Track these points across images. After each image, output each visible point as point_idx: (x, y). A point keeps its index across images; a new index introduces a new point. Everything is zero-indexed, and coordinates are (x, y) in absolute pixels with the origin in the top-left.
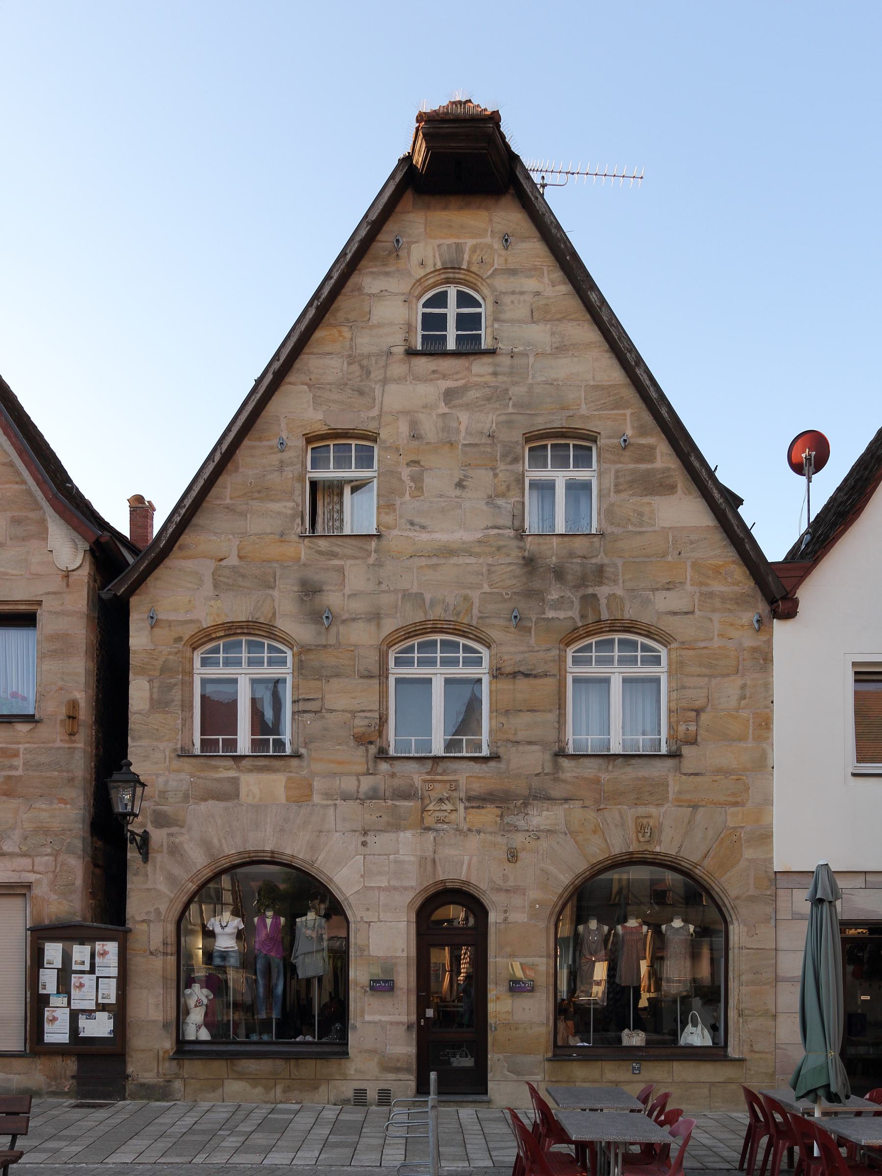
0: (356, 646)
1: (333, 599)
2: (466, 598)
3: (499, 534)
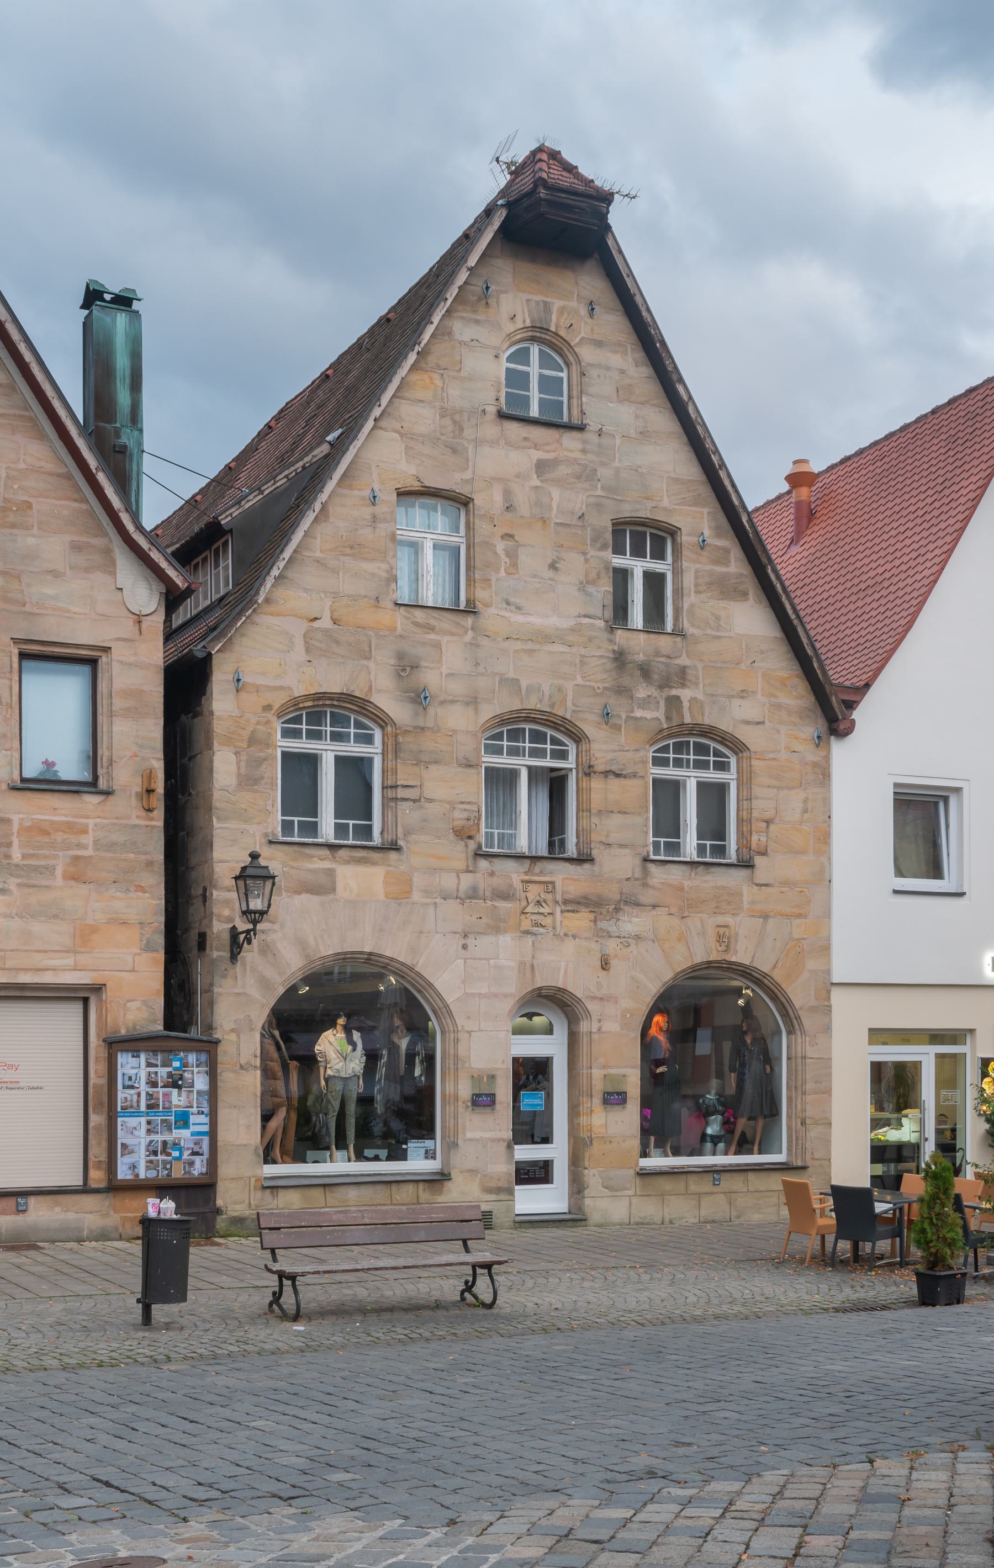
0: (455, 731)
1: (431, 678)
2: (560, 689)
3: (592, 625)
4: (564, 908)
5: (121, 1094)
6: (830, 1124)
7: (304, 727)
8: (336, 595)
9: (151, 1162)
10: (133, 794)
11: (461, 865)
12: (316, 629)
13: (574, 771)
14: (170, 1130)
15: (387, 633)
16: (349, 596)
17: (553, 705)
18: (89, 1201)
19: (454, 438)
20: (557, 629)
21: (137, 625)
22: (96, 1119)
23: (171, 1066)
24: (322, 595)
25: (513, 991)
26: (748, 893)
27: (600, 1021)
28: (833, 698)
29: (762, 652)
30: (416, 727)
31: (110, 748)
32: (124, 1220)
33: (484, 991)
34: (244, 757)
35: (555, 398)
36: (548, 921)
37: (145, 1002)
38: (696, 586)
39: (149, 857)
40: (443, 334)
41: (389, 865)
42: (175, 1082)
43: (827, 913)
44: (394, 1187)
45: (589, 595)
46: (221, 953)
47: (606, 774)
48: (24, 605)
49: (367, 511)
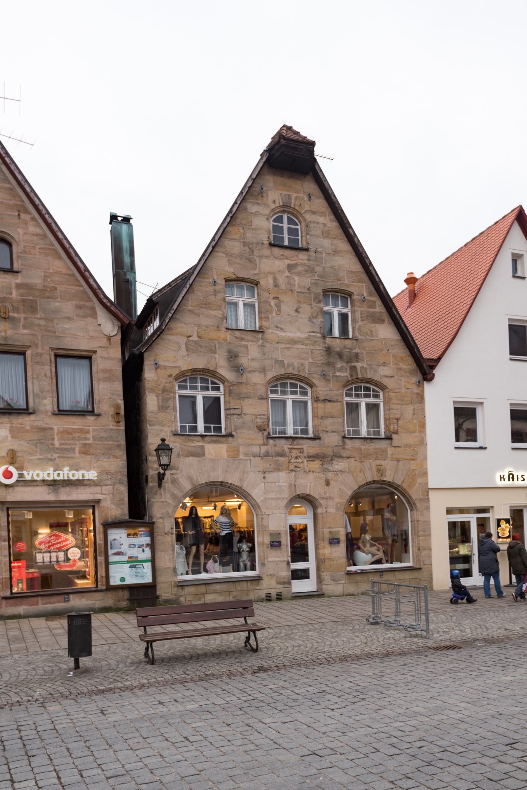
0: (255, 384)
1: (243, 361)
2: (302, 364)
3: (315, 336)
6: (431, 549)
7: (188, 384)
8: (199, 326)
10: (110, 415)
11: (261, 442)
16: (205, 326)
17: (299, 371)
18: (98, 595)
19: (250, 255)
20: (300, 338)
24: (193, 326)
25: (287, 496)
26: (390, 451)
27: (326, 508)
28: (424, 365)
29: (392, 346)
30: (238, 383)
33: (274, 496)
34: (160, 398)
36: (302, 465)
38: (361, 317)
39: (118, 443)
40: (243, 210)
43: (425, 459)
44: (237, 583)
47: (324, 401)
48: (55, 332)
49: (212, 289)
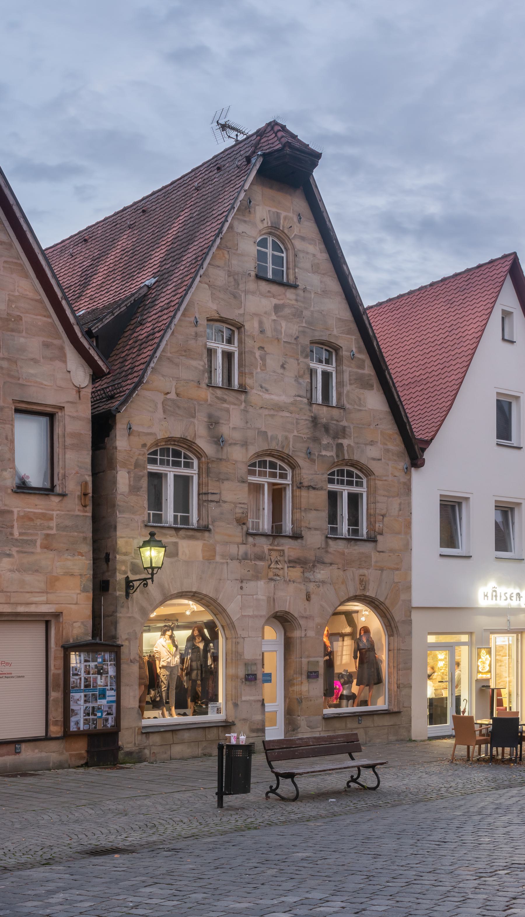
0: (236, 461)
1: (225, 430)
2: (287, 438)
3: (301, 401)
4: (289, 565)
5: (73, 679)
6: (411, 687)
7: (159, 457)
8: (178, 379)
9: (86, 720)
10: (76, 496)
11: (239, 540)
12: (168, 399)
13: (290, 486)
14: (96, 700)
15: (203, 402)
16: (185, 380)
17: (283, 447)
18: (53, 745)
20: (285, 403)
21: (78, 394)
22: (56, 695)
23: (96, 661)
24: (171, 379)
26: (375, 557)
27: (306, 630)
29: (380, 419)
30: (217, 459)
31: (64, 468)
32: (71, 755)
33: (251, 614)
34: (132, 475)
35: (280, 268)
36: (281, 573)
37: (82, 623)
38: (350, 380)
41: (205, 540)
42: (100, 671)
43: (410, 568)
44: (207, 730)
45: (299, 383)
46: (121, 593)
47: (309, 487)
48: (19, 379)
49: (192, 330)
